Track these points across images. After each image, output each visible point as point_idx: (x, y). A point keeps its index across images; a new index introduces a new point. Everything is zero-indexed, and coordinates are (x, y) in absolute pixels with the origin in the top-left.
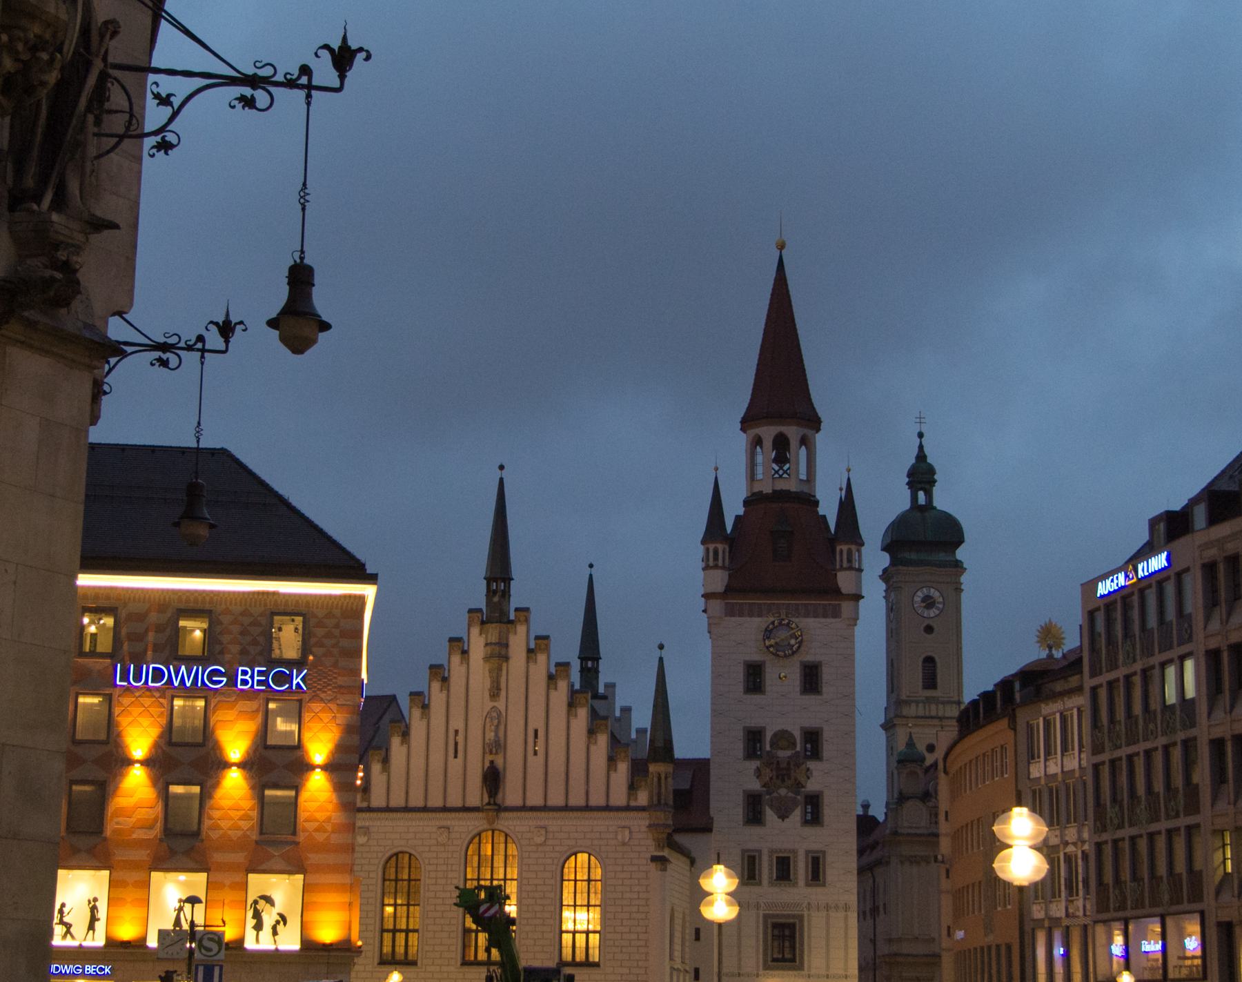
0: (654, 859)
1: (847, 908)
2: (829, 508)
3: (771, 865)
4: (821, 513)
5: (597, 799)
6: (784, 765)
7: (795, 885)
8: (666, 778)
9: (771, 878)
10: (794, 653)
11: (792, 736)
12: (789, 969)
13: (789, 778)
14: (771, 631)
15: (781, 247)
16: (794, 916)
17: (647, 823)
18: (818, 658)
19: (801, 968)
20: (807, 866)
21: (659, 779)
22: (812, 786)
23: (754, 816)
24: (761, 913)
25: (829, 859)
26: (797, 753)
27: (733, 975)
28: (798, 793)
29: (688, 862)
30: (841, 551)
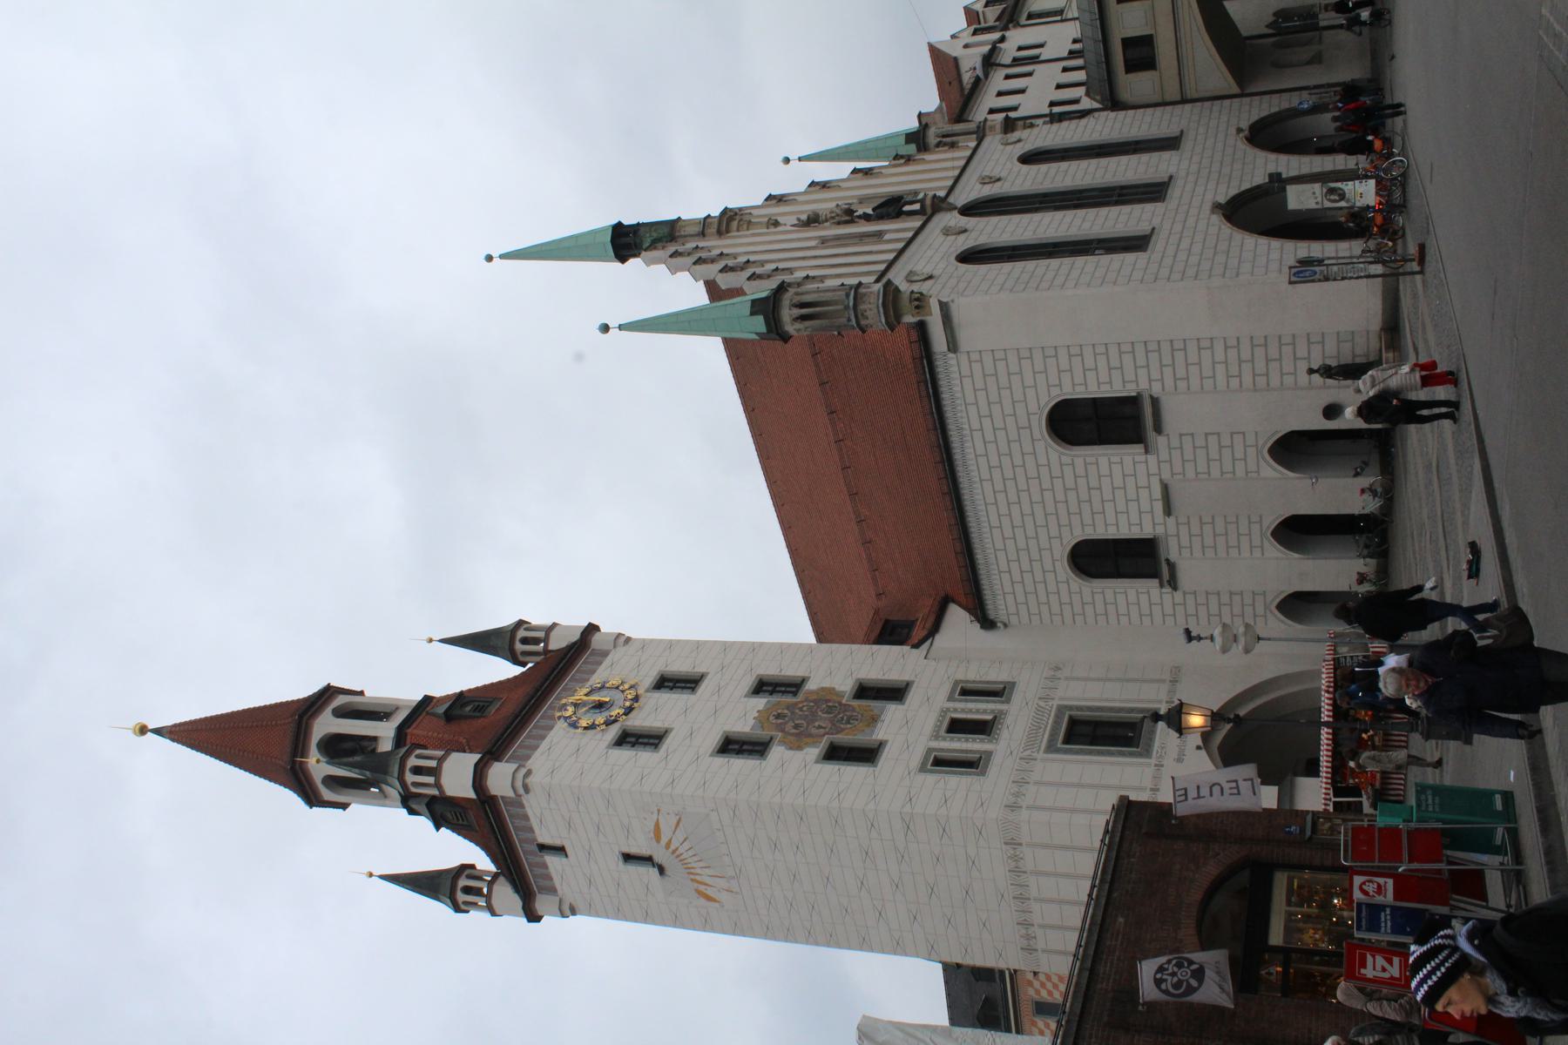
9: (982, 741)
15: (143, 730)
24: (1041, 755)
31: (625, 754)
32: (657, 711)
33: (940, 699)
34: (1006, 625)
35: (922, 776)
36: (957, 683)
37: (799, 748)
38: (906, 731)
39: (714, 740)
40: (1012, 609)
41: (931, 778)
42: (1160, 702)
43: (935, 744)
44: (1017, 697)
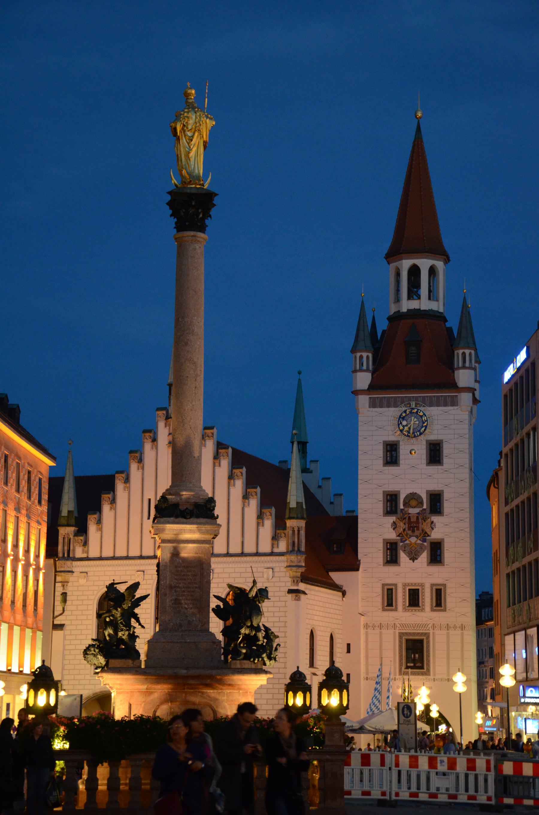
0: (290, 591)
1: (462, 627)
2: (453, 323)
3: (404, 595)
4: (448, 325)
5: (250, 548)
6: (413, 519)
7: (423, 610)
8: (299, 531)
9: (403, 605)
10: (421, 434)
11: (420, 497)
12: (418, 674)
13: (418, 529)
14: (403, 418)
16: (422, 634)
17: (285, 564)
18: (440, 437)
19: (428, 673)
20: (432, 596)
21: (293, 531)
22: (435, 535)
23: (392, 558)
24: (397, 632)
25: (448, 591)
26: (424, 509)
28: (424, 541)
29: (340, 594)
30: (458, 354)
35: (380, 586)
41: (380, 590)
42: (434, 675)
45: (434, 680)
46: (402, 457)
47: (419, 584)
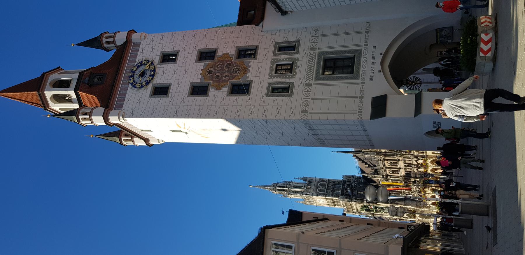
9: (289, 77)
16: (318, 59)
18: (159, 54)
24: (313, 82)
27: (361, 102)
31: (156, 99)
32: (164, 74)
33: (270, 56)
34: (291, 12)
35: (268, 99)
36: (276, 43)
37: (218, 89)
38: (259, 73)
39: (187, 89)
40: (293, 6)
41: (272, 99)
42: (361, 45)
43: (271, 81)
44: (301, 50)
45: (366, 45)
46: (165, 82)
47: (271, 64)
